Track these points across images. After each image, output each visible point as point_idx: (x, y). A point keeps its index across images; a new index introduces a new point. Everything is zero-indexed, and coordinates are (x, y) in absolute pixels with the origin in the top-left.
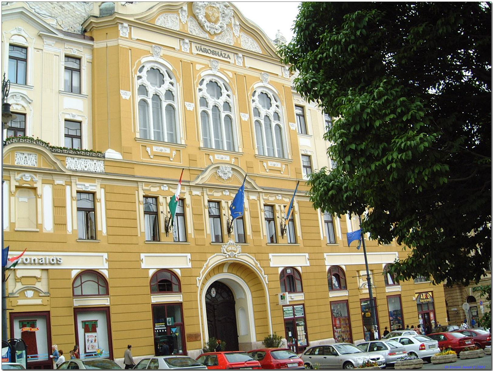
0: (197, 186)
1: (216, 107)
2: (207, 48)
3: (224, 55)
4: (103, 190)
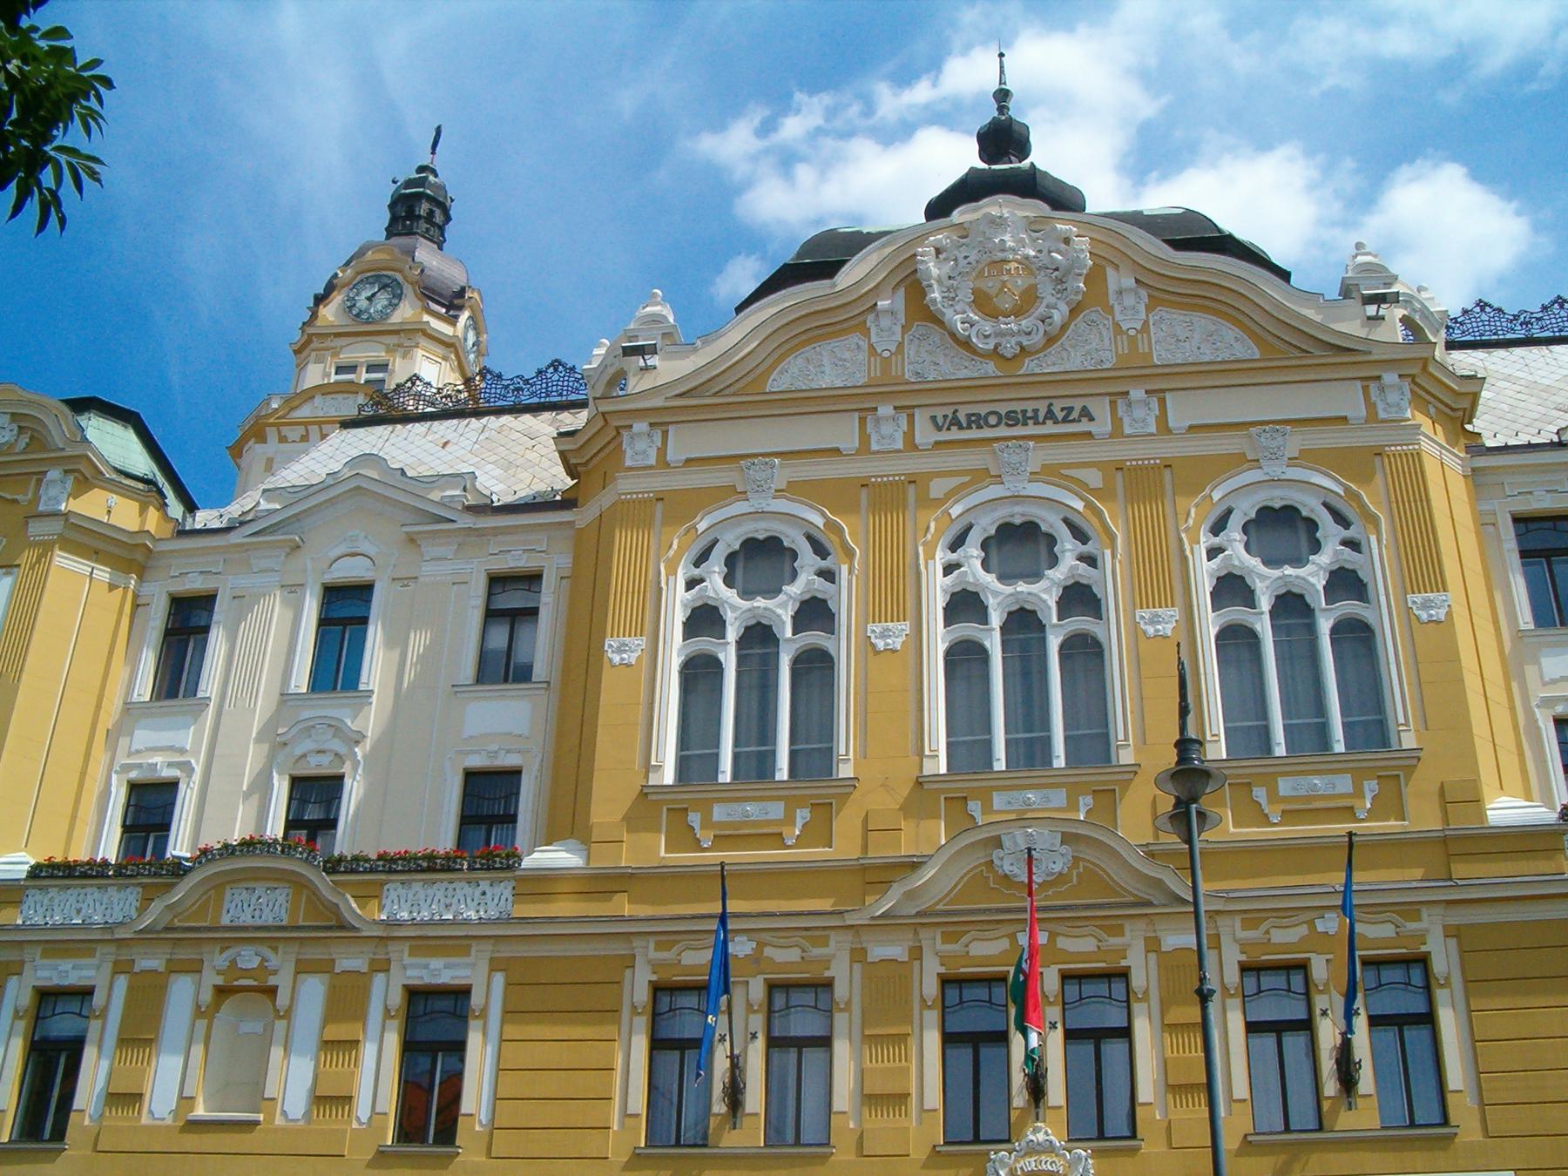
0: (887, 923)
3: (1060, 415)
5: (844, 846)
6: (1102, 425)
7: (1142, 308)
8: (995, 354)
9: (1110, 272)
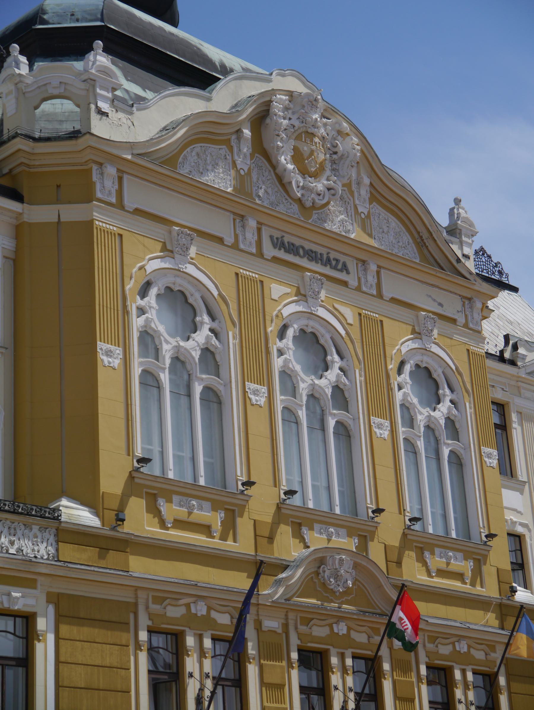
1: (313, 397)
3: (334, 263)
4: (51, 609)
5: (243, 545)
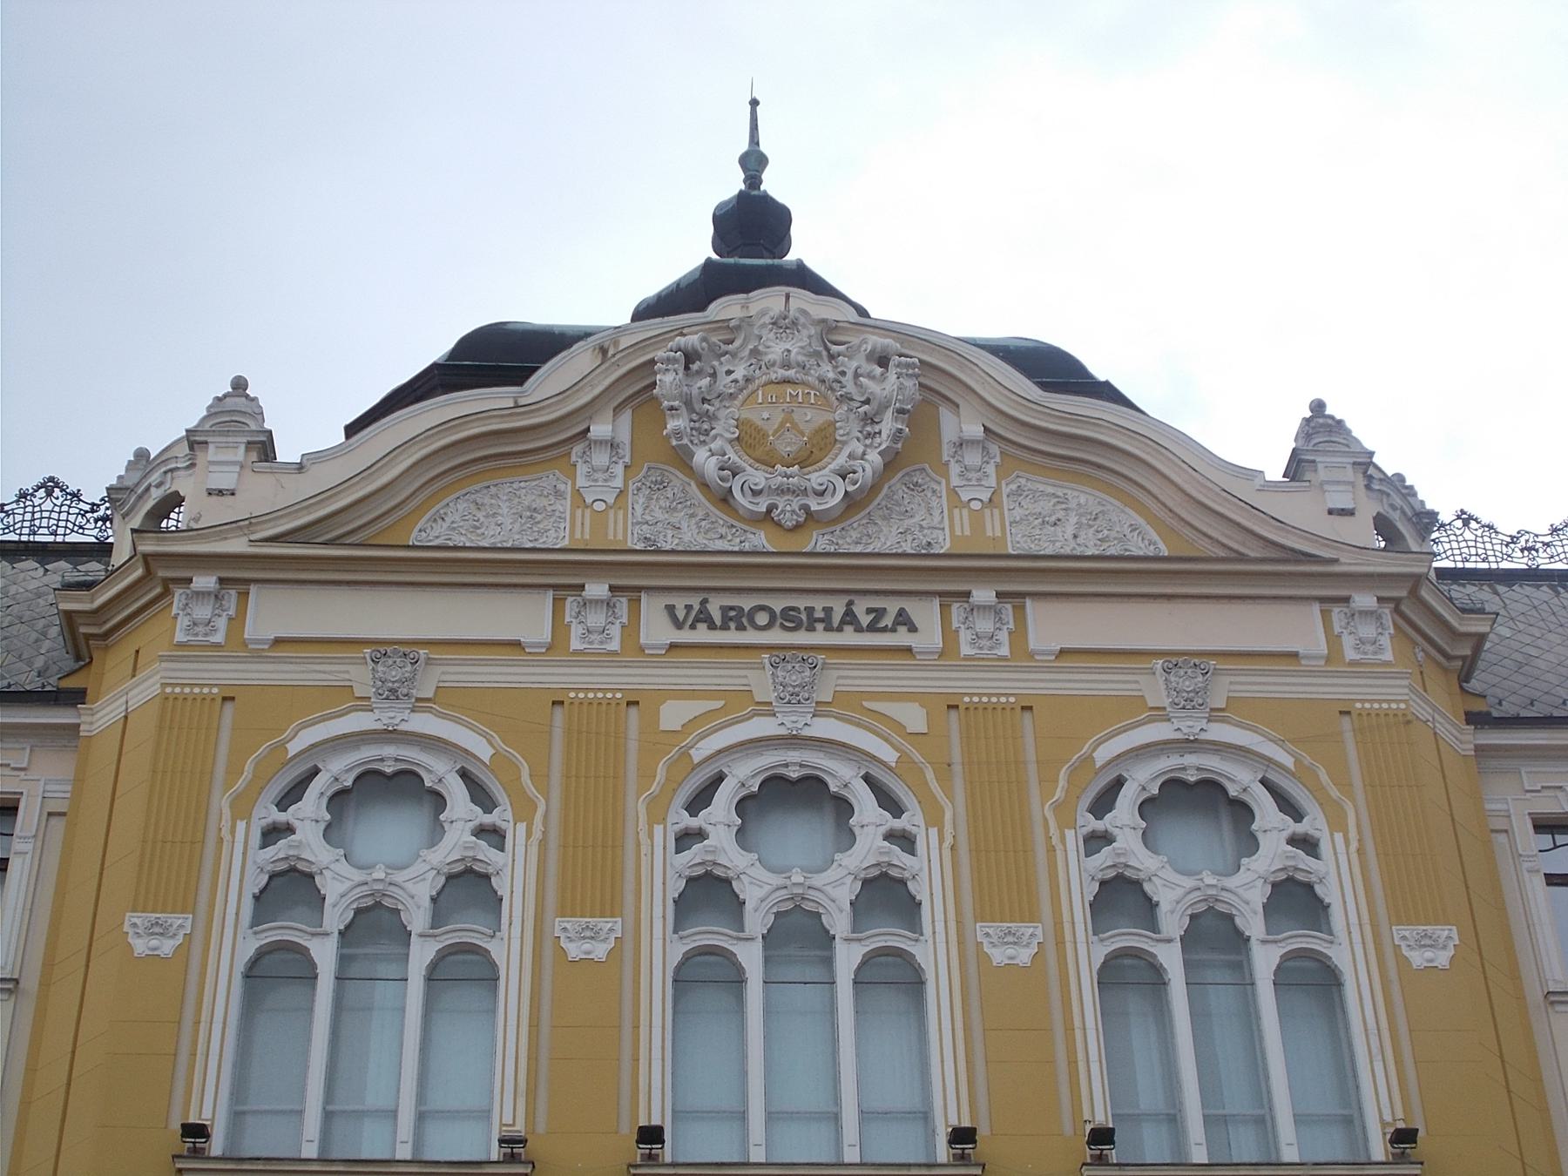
2: (747, 603)
3: (865, 620)
6: (929, 636)
7: (991, 469)
8: (767, 517)
9: (945, 414)
